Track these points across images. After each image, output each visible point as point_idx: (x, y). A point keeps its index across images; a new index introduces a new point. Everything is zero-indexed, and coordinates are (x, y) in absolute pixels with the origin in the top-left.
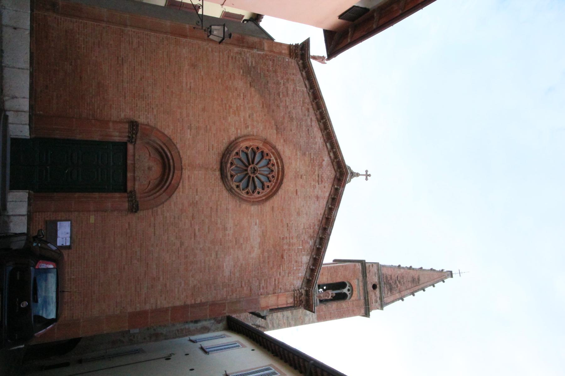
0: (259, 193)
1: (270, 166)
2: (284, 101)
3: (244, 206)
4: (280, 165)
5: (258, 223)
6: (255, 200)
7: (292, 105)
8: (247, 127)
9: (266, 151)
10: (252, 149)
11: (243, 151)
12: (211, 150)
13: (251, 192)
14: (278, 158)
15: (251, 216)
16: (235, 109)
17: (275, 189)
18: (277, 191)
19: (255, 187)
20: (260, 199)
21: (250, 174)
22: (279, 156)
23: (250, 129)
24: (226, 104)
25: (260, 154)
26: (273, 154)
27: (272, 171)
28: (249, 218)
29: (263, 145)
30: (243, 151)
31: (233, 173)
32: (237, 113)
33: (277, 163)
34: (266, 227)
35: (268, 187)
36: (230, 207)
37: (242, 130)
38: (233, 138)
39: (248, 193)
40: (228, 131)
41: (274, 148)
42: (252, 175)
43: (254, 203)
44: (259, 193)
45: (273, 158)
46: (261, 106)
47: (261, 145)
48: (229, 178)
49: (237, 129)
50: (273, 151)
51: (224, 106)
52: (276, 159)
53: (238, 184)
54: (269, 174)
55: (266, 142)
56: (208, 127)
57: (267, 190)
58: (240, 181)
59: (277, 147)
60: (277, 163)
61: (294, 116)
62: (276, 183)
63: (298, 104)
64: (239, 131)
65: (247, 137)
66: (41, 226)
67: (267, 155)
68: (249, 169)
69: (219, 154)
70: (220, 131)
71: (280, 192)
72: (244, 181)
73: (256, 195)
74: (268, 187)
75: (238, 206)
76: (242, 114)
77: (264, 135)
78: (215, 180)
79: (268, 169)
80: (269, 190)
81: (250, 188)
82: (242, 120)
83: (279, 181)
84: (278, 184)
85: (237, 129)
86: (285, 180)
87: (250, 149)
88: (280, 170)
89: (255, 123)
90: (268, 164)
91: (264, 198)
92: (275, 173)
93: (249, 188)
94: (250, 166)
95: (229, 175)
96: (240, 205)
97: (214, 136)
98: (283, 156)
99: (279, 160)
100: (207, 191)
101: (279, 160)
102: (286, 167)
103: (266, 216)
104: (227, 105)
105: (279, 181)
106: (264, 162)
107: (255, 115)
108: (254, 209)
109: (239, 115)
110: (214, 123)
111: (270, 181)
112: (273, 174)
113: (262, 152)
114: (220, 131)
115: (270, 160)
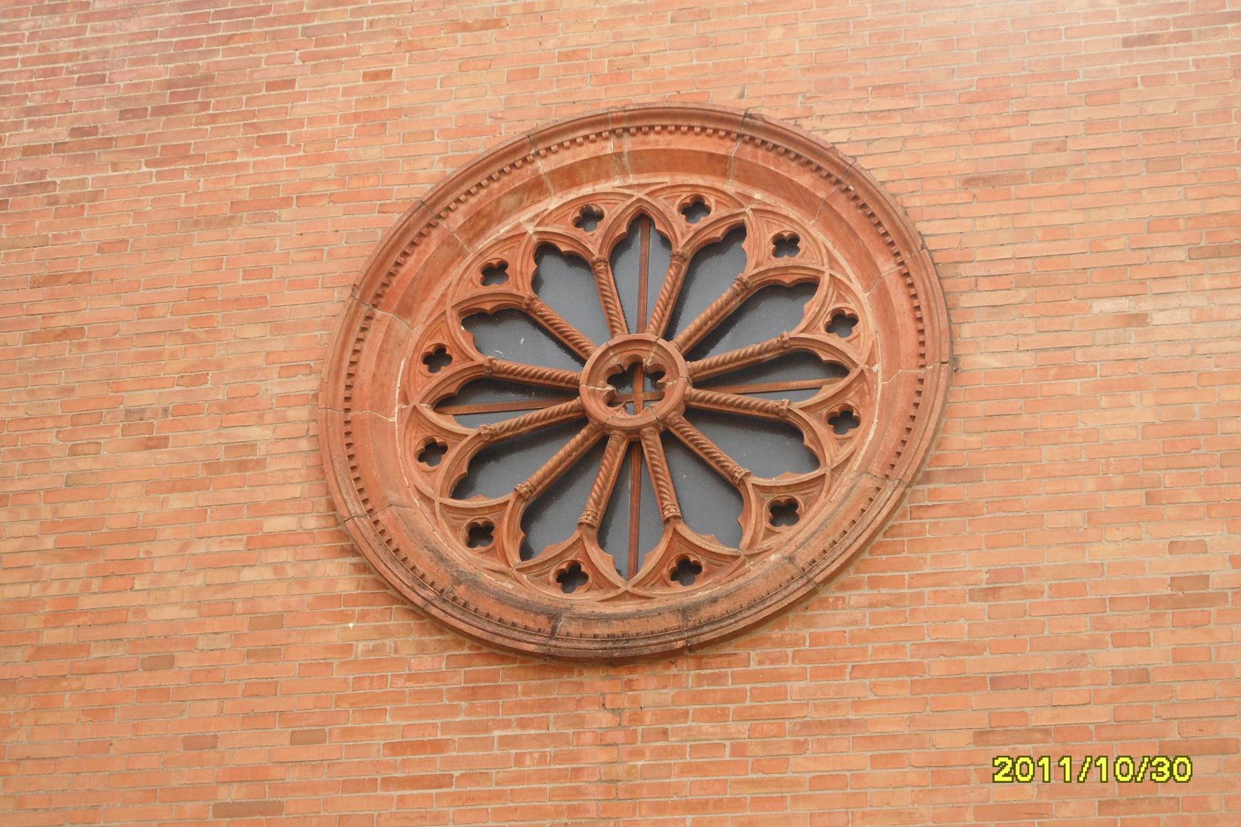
0: (842, 321)
1: (593, 241)
2: (32, 164)
3: (961, 441)
4: (586, 152)
5: (1124, 305)
6: (908, 343)
7: (72, 93)
8: (245, 461)
9: (461, 283)
10: (442, 404)
11: (461, 488)
12: (436, 765)
13: (811, 306)
14: (525, 175)
15: (1066, 371)
16: (81, 568)
17: (805, 180)
18: (811, 155)
19: (798, 357)
20: (899, 299)
21: (666, 407)
22: (506, 166)
23: (254, 433)
24: (40, 652)
25: (489, 333)
26: (480, 222)
27: (642, 219)
28: (1075, 386)
29: (406, 310)
30: (461, 488)
31: (654, 556)
32: (128, 551)
33: (568, 176)
34: (1166, 224)
35: (785, 244)
36: (971, 563)
37: (264, 495)
38: (338, 575)
39: (844, 419)
40: (276, 621)
41: (429, 212)
42: (678, 387)
43: (937, 360)
44: (842, 321)
45: (526, 221)
46: (65, 349)
47: (414, 334)
48: (700, 590)
49: (260, 542)
50: (458, 219)
51: (45, 667)
52: (536, 188)
53: (757, 513)
54: (666, 242)
55: (378, 287)
56: (230, 794)
57: (820, 249)
58: (733, 487)
59: (424, 189)
60: (568, 176)
61: (163, 71)
62: (749, 175)
63: (64, 46)
64: (275, 524)
65: (342, 443)
66: (902, 685)
67: (494, 271)
68: (618, 417)
69: (472, 693)
70: (272, 687)
71: (833, 131)
72: (732, 451)
73: (853, 348)
74: (785, 244)
75: (965, 492)
76: (130, 504)
77: (321, 307)
78: (717, 716)
79: (629, 262)
80: (814, 233)
81: (800, 397)
82: (176, 502)
83: (731, 149)
84: (761, 159)
85: (260, 542)
86: (725, 99)
87: (446, 422)
88: (628, 144)
89: (213, 391)
90: (576, 260)
91: (887, 268)
92: (663, 190)
93: (795, 405)
94: (599, 410)
95: (679, 594)
96: (956, 474)
97: (312, 738)
98: (509, 133)
99: (543, 166)
100: (819, 781)
101: (543, 166)
102: (611, 99)
103: (1053, 233)
104: (51, 637)
105: (731, 149)
106: (565, 300)
107: (143, 398)
108: (991, 351)
109: (132, 534)
110: (200, 744)
111: (737, 232)
112: (670, 208)
113: (473, 317)
114: (272, 687)
115: (545, 249)
